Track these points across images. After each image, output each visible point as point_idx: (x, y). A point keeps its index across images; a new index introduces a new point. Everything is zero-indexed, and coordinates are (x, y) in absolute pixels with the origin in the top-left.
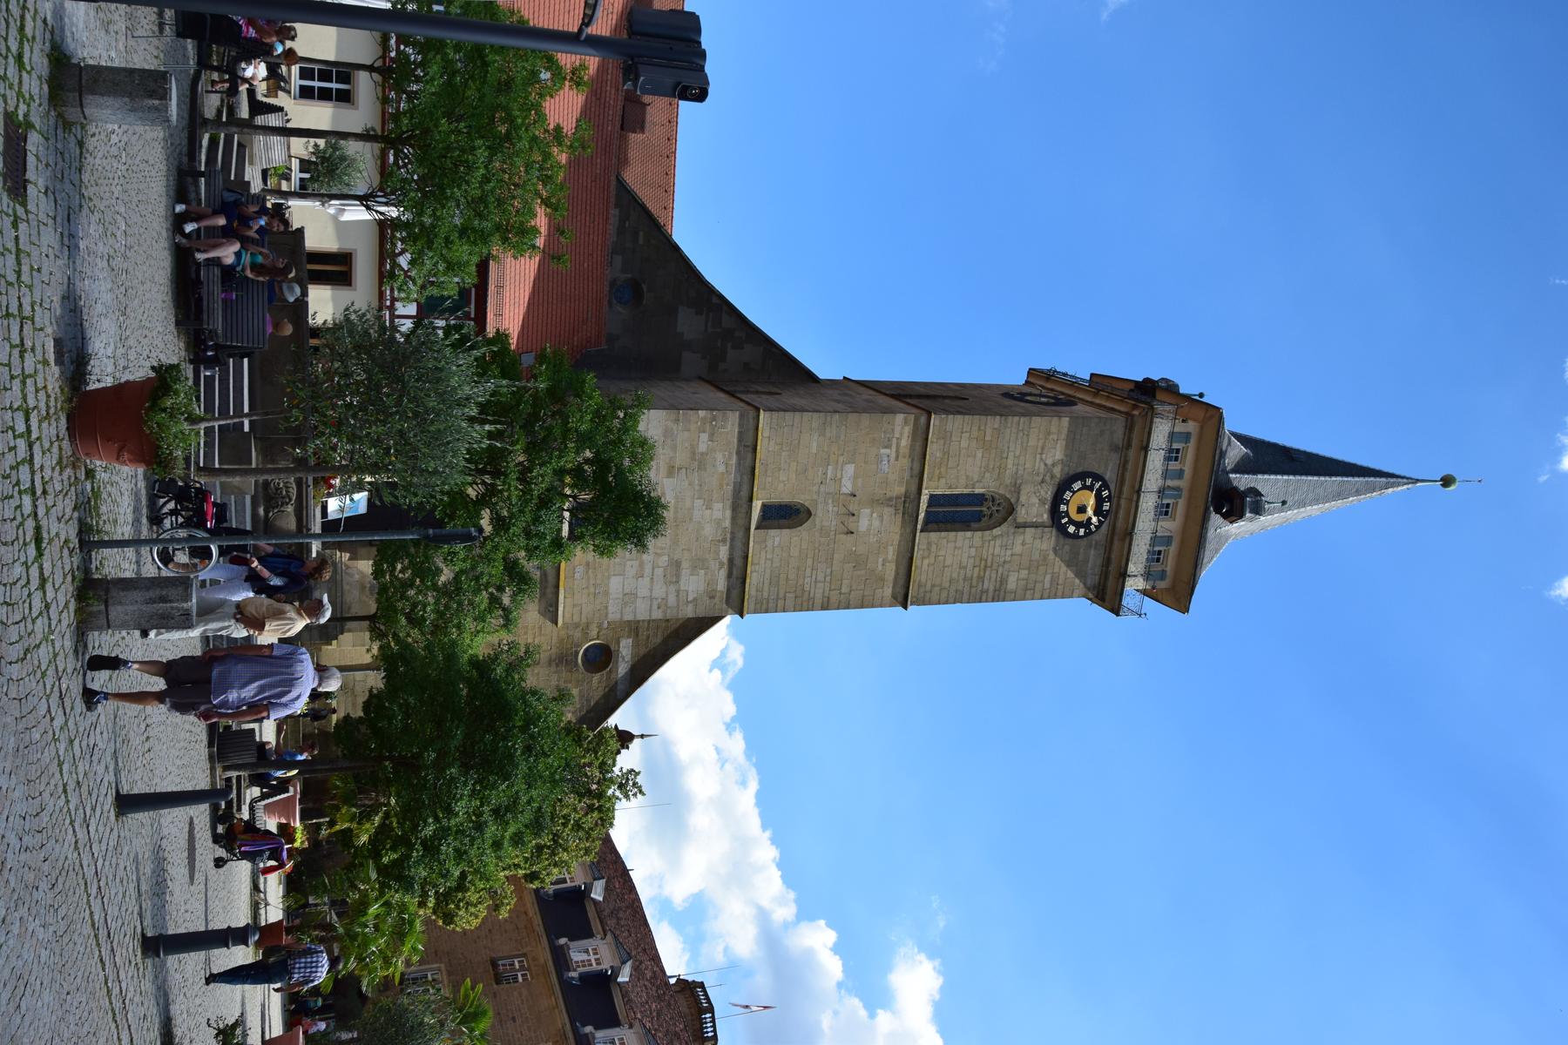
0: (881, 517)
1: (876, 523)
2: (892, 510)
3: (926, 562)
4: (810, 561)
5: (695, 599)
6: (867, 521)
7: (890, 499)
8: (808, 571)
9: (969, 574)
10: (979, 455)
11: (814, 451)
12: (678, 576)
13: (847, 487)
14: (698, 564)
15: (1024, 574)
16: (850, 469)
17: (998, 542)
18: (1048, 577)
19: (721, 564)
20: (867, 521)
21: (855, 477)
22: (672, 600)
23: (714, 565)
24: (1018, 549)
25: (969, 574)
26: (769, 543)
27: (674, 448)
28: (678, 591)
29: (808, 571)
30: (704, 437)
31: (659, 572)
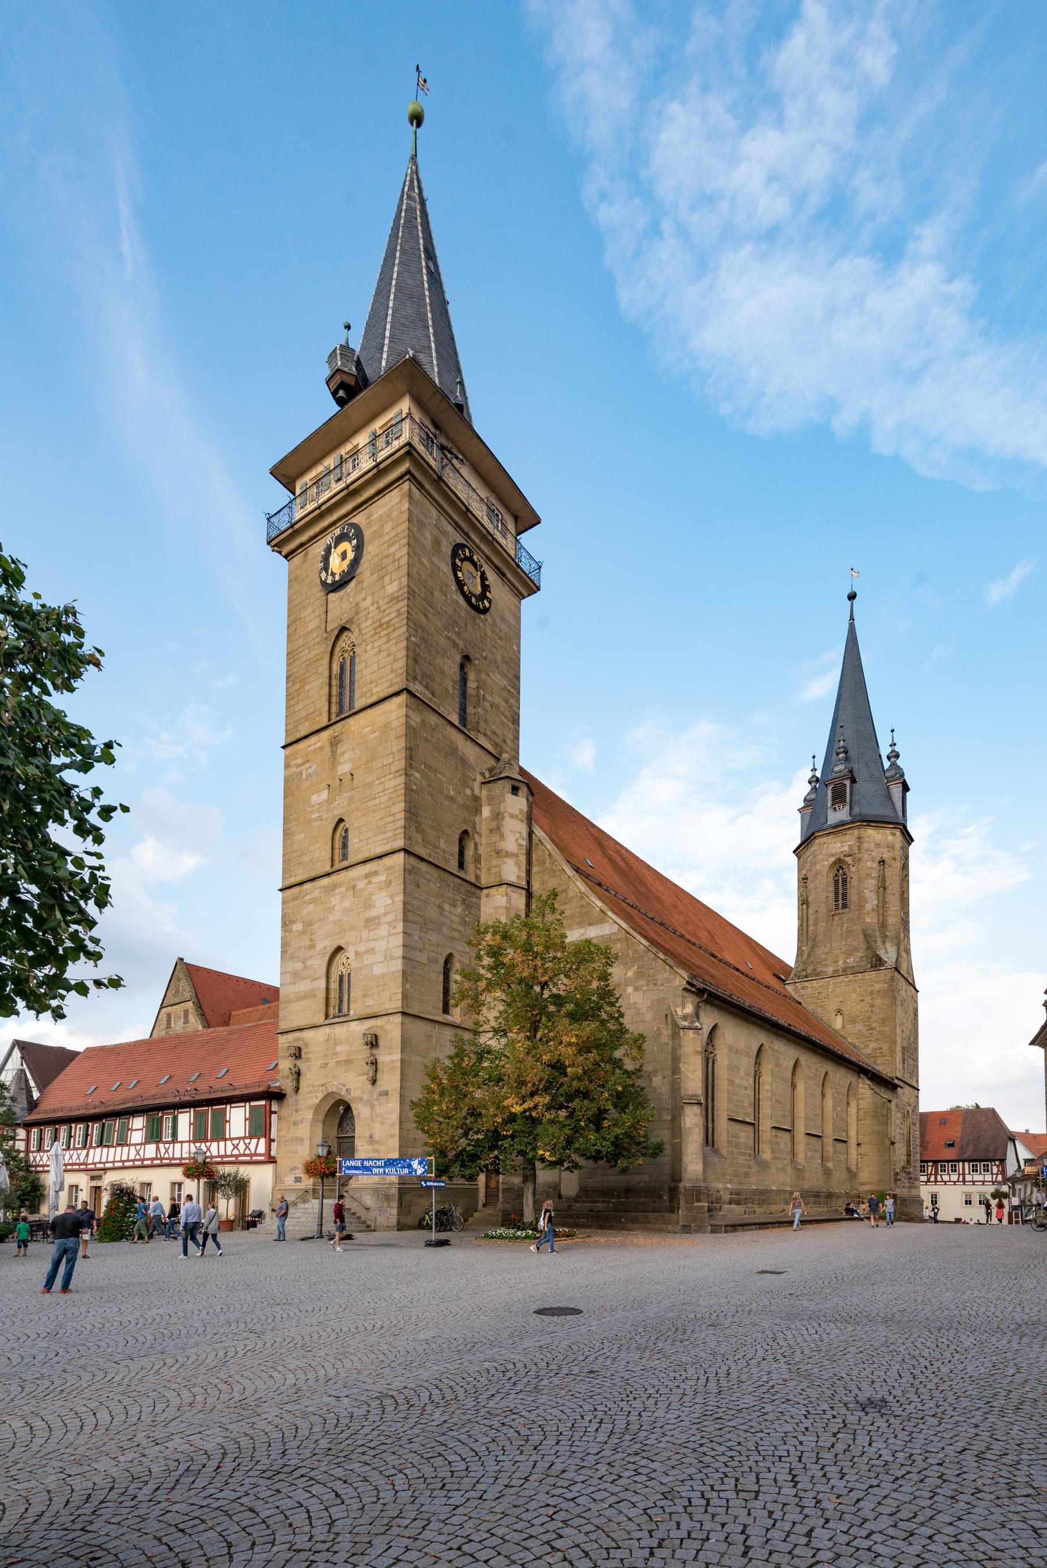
0: (343, 754)
1: (347, 756)
2: (339, 746)
6: (344, 768)
12: (375, 918)
14: (368, 904)
20: (344, 768)
26: (356, 846)
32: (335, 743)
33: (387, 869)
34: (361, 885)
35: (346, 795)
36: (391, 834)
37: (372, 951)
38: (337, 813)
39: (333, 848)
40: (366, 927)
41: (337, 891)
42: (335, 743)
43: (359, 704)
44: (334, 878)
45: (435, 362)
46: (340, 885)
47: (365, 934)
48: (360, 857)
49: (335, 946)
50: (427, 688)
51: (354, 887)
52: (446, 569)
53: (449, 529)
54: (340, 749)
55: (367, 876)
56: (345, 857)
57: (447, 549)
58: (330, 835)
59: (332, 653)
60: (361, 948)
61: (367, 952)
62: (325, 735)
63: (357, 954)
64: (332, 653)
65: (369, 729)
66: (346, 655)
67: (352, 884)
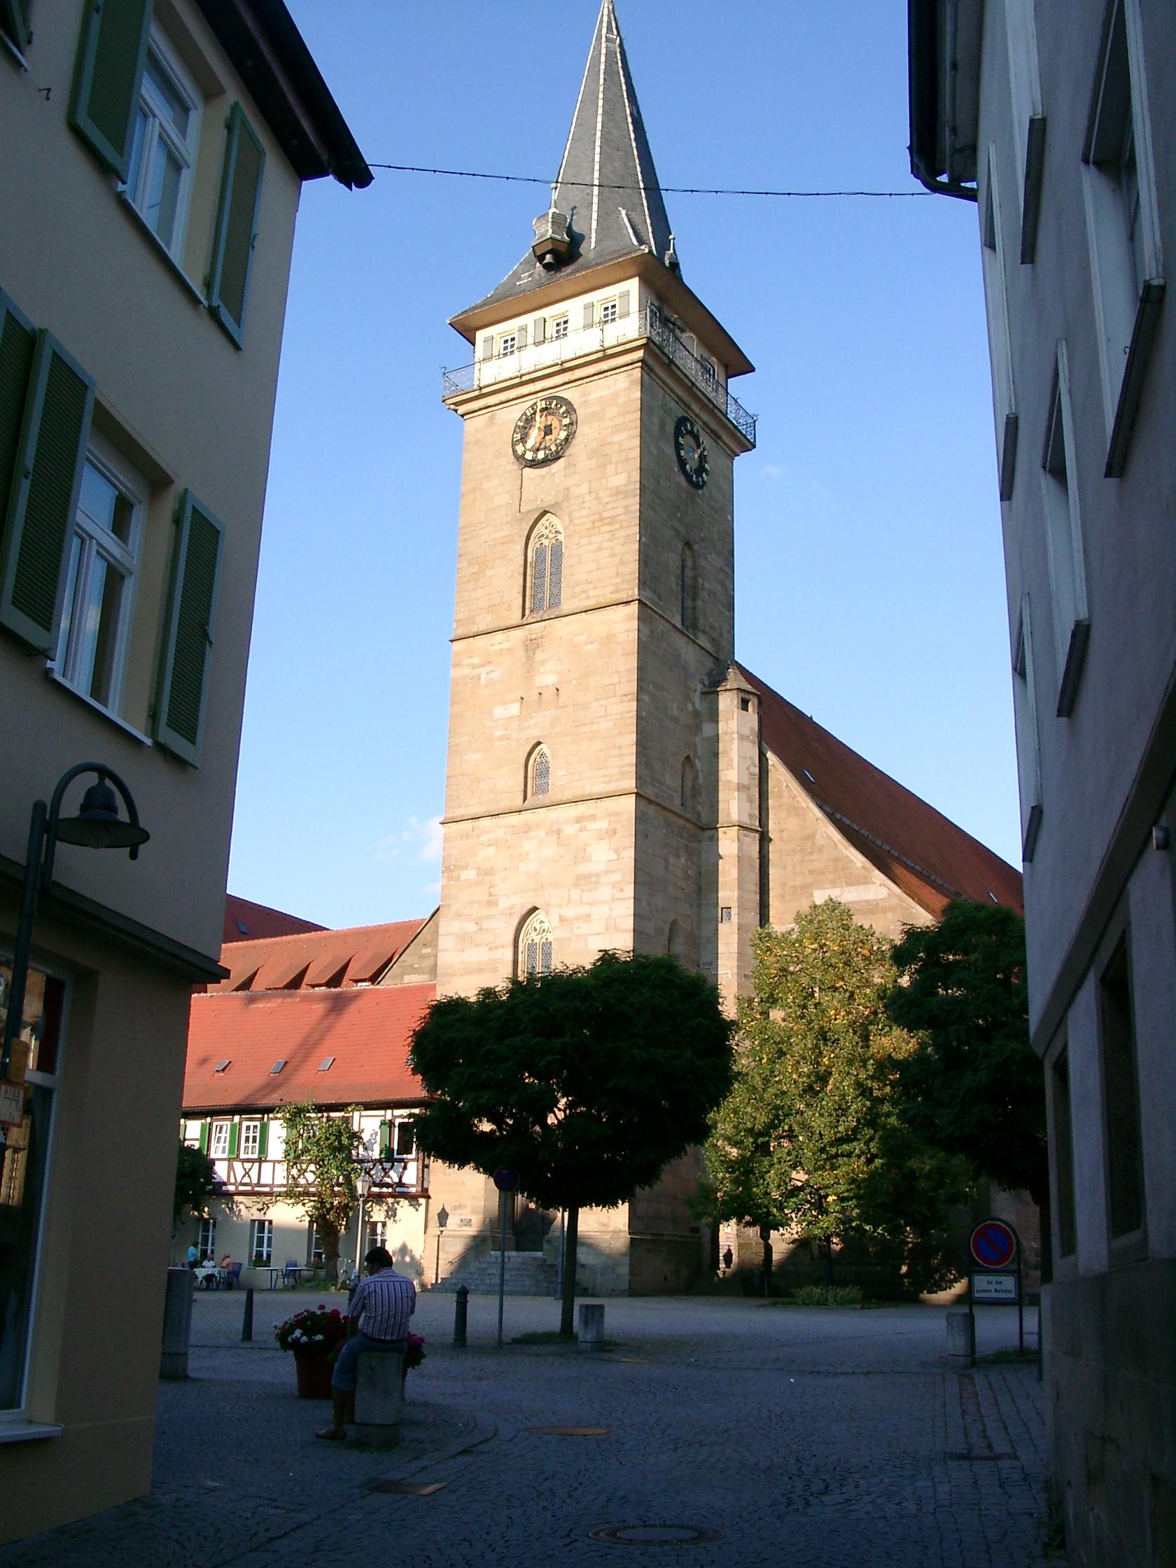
0: (543, 662)
1: (550, 665)
3: (592, 593)
4: (585, 729)
5: (617, 851)
6: (546, 678)
7: (528, 658)
8: (594, 728)
9: (607, 536)
10: (489, 572)
11: (479, 755)
12: (590, 875)
13: (515, 709)
14: (581, 856)
15: (610, 469)
16: (499, 712)
17: (576, 515)
18: (617, 438)
19: (583, 829)
20: (546, 678)
21: (505, 703)
22: (615, 877)
23: (584, 836)
24: (584, 489)
25: (607, 536)
27: (471, 903)
28: (607, 872)
29: (594, 728)
30: (464, 875)
31: (587, 897)
32: (531, 646)
33: (610, 815)
34: (570, 830)
35: (547, 713)
36: (616, 771)
37: (587, 918)
38: (534, 734)
39: (526, 777)
40: (576, 885)
41: (532, 834)
42: (531, 646)
43: (566, 606)
44: (528, 816)
45: (648, 221)
46: (538, 826)
47: (575, 894)
48: (568, 795)
49: (529, 907)
50: (654, 592)
51: (559, 832)
52: (670, 450)
53: (672, 405)
54: (539, 656)
55: (579, 820)
56: (543, 789)
57: (670, 429)
58: (523, 761)
59: (528, 538)
60: (570, 913)
61: (578, 918)
62: (518, 633)
63: (562, 919)
64: (528, 538)
65: (584, 638)
66: (546, 542)
67: (555, 827)
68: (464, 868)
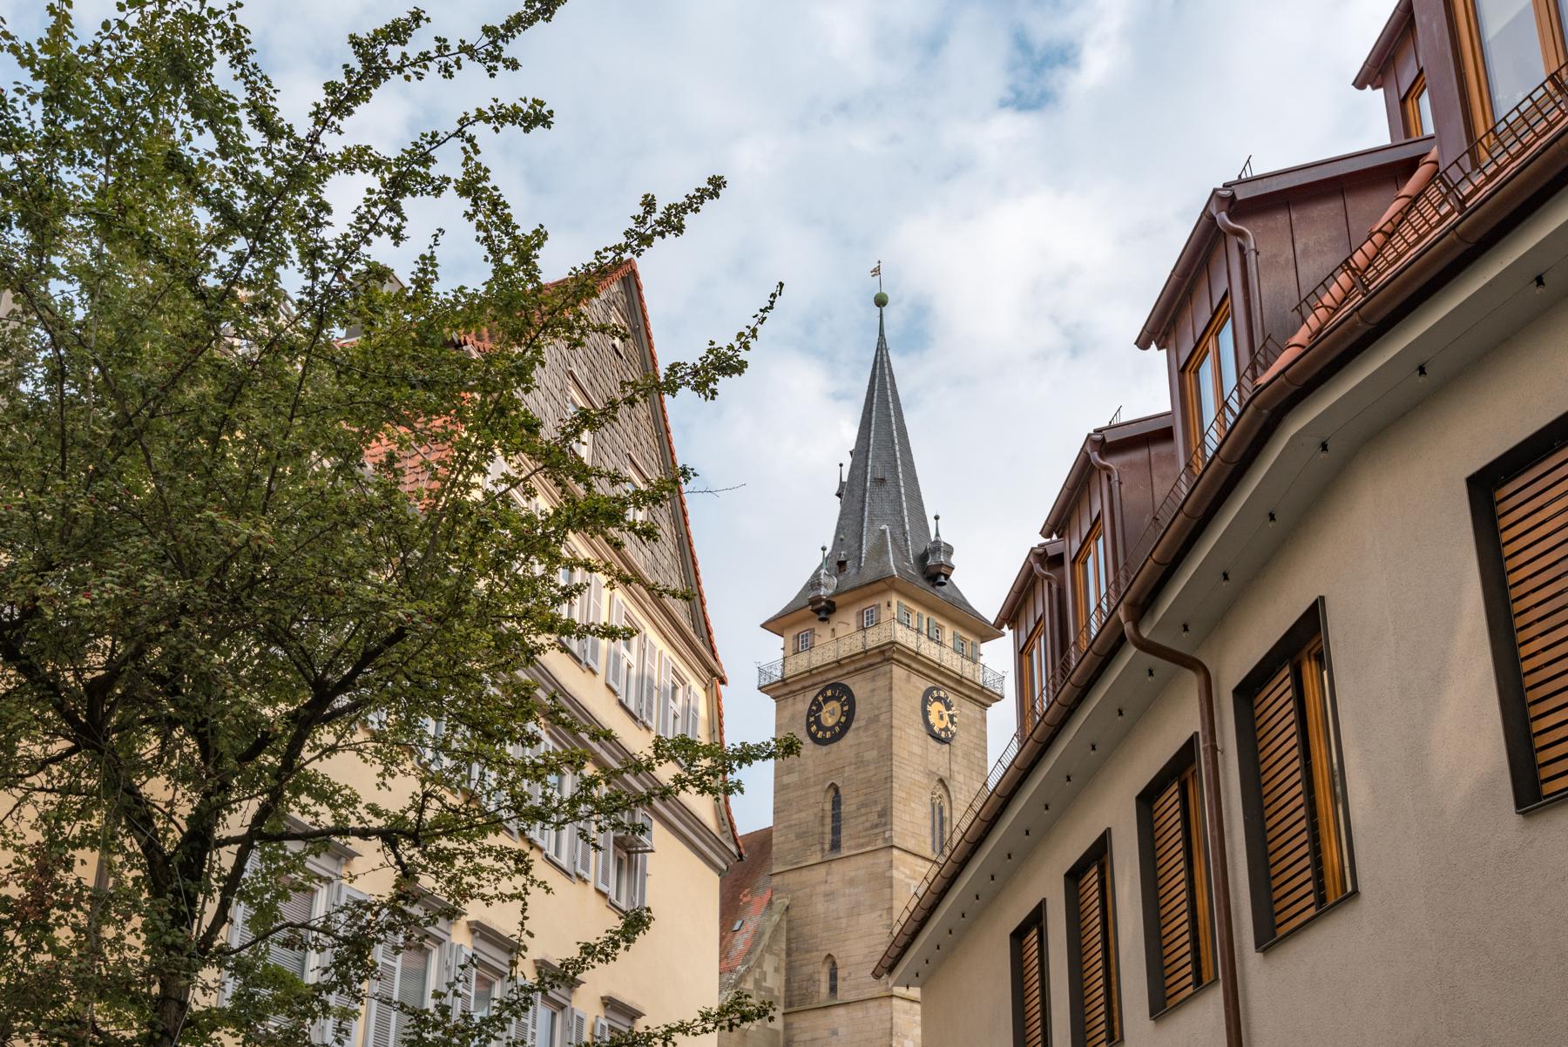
68: (906, 1037)
